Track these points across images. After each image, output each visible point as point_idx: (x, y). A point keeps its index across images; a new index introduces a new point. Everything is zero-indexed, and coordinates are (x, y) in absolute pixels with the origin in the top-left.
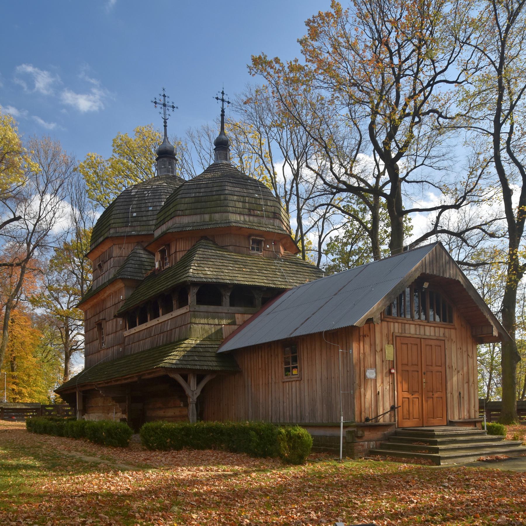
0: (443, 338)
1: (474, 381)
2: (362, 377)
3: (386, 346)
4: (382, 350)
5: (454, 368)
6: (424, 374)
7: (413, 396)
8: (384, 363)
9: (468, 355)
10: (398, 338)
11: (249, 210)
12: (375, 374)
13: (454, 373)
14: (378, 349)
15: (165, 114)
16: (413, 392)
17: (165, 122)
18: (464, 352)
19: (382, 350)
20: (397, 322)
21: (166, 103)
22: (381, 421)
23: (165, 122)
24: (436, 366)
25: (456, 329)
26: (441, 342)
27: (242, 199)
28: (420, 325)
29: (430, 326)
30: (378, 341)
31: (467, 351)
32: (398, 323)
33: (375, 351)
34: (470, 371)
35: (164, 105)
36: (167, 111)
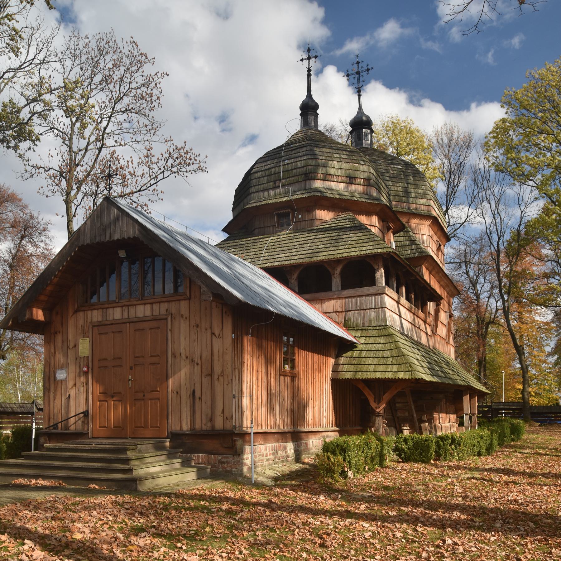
0: (164, 317)
1: (223, 372)
2: (52, 379)
3: (81, 341)
4: (75, 346)
5: (183, 356)
6: (131, 368)
7: (114, 399)
8: (78, 361)
9: (213, 334)
10: (96, 329)
11: (275, 182)
12: (65, 375)
13: (183, 363)
14: (71, 345)
16: (114, 393)
18: (203, 330)
19: (75, 346)
22: (72, 428)
24: (152, 356)
25: (190, 299)
27: (267, 173)
28: (128, 306)
29: (145, 304)
30: (71, 336)
31: (211, 328)
32: (98, 309)
33: (68, 347)
34: (216, 357)
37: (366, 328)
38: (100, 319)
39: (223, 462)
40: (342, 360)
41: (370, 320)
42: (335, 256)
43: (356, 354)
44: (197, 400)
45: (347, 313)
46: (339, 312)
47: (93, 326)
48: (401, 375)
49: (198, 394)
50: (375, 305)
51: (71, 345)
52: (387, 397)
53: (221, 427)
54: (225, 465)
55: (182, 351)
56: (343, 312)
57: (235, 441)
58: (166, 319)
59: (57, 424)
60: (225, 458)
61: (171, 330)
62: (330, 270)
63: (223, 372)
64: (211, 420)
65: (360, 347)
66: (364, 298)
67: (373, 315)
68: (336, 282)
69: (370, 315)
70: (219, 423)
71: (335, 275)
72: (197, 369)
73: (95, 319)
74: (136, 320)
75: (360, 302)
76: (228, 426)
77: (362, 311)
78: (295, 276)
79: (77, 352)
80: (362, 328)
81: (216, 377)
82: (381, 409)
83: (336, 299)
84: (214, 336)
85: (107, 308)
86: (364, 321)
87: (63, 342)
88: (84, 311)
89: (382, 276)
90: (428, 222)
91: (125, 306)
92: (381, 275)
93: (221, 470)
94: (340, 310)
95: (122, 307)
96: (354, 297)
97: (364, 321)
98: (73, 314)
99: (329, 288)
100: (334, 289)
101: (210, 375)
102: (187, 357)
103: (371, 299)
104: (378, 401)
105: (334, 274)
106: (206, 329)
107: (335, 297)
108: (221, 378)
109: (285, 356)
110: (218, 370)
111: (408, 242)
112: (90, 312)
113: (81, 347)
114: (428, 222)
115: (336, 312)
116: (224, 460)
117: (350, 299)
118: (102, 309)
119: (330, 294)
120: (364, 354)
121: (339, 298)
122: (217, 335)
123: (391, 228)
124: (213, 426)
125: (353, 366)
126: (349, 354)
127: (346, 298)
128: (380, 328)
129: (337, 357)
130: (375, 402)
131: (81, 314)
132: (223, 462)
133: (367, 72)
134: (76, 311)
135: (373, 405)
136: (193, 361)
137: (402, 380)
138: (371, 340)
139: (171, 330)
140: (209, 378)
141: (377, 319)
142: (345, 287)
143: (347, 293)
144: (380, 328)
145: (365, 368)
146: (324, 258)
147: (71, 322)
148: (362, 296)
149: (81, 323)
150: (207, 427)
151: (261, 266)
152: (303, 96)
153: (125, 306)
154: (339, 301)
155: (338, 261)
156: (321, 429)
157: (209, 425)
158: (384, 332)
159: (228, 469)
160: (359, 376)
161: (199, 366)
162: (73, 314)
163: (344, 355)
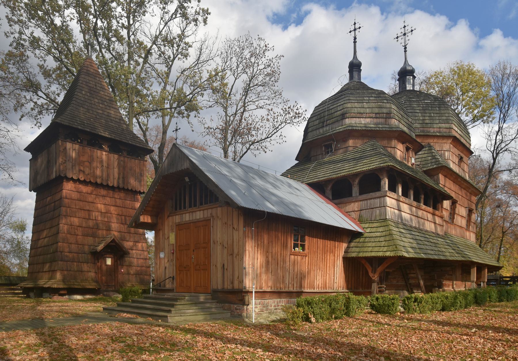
4: (168, 238)
5: (219, 243)
6: (194, 251)
9: (234, 228)
14: (166, 237)
15: (405, 42)
17: (405, 48)
19: (168, 238)
20: (177, 215)
21: (402, 34)
23: (405, 48)
24: (203, 243)
26: (206, 223)
27: (319, 117)
29: (200, 211)
30: (166, 231)
31: (233, 224)
33: (165, 238)
34: (235, 244)
35: (405, 34)
36: (407, 38)
37: (373, 222)
38: (179, 221)
39: (237, 309)
40: (352, 244)
41: (375, 216)
42: (352, 172)
43: (362, 240)
44: (225, 270)
45: (361, 212)
46: (356, 211)
47: (176, 225)
48: (388, 254)
49: (226, 267)
50: (380, 205)
51: (166, 237)
52: (380, 269)
53: (237, 288)
54: (238, 311)
55: (218, 239)
56: (358, 211)
57: (244, 296)
58: (210, 220)
59: (160, 283)
60: (239, 306)
61: (213, 227)
62: (351, 182)
63: (238, 252)
64: (232, 283)
65: (366, 235)
66: (373, 200)
67: (378, 211)
68: (355, 190)
69: (376, 212)
70: (236, 286)
71: (355, 185)
72: (225, 251)
73: (177, 221)
74: (196, 221)
75: (370, 203)
76: (241, 288)
77: (371, 210)
78: (329, 187)
79: (169, 241)
80: (370, 222)
81: (235, 256)
82: (375, 277)
83: (354, 202)
84: (234, 230)
85: (183, 214)
86: (371, 216)
87: (163, 235)
88: (172, 216)
89: (385, 184)
90: (450, 141)
91: (190, 212)
92: (385, 183)
93: (236, 314)
94: (356, 210)
95: (189, 213)
96: (366, 200)
97: (371, 216)
98: (167, 218)
99: (350, 195)
100: (353, 195)
101: (232, 255)
102: (220, 244)
103: (377, 201)
104: (374, 272)
105: (354, 185)
106: (230, 225)
107: (354, 200)
108: (237, 256)
109: (295, 242)
110: (236, 251)
111: (430, 158)
112: (174, 217)
113: (170, 239)
114: (450, 141)
115: (354, 211)
116: (238, 308)
117: (364, 202)
118: (180, 214)
119: (350, 199)
120: (367, 240)
121: (357, 201)
122: (236, 229)
123: (411, 148)
124: (233, 287)
125: (358, 248)
126: (357, 240)
127: (361, 201)
128: (382, 221)
129: (350, 242)
130: (372, 272)
131: (171, 218)
132: (237, 309)
133: (411, 33)
134: (168, 216)
135: (371, 275)
136: (223, 246)
137: (390, 257)
138: (374, 230)
139: (213, 227)
140: (231, 256)
141: (380, 215)
142: (361, 193)
143: (364, 196)
144: (382, 221)
145: (365, 249)
146: (345, 174)
147: (166, 223)
148: (371, 199)
149: (171, 224)
150: (230, 287)
151: (306, 182)
152: (351, 58)
153: (190, 212)
154: (356, 204)
155: (356, 175)
156: (330, 291)
157: (231, 286)
158: (383, 224)
159: (240, 313)
160: (361, 255)
161: (227, 249)
162: (167, 218)
163: (354, 241)
